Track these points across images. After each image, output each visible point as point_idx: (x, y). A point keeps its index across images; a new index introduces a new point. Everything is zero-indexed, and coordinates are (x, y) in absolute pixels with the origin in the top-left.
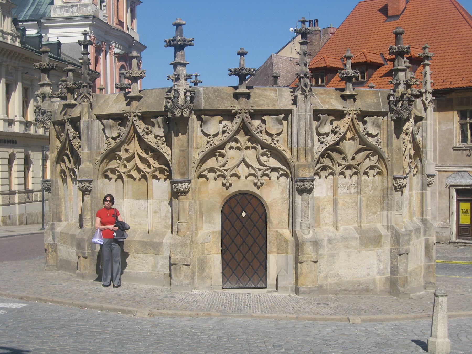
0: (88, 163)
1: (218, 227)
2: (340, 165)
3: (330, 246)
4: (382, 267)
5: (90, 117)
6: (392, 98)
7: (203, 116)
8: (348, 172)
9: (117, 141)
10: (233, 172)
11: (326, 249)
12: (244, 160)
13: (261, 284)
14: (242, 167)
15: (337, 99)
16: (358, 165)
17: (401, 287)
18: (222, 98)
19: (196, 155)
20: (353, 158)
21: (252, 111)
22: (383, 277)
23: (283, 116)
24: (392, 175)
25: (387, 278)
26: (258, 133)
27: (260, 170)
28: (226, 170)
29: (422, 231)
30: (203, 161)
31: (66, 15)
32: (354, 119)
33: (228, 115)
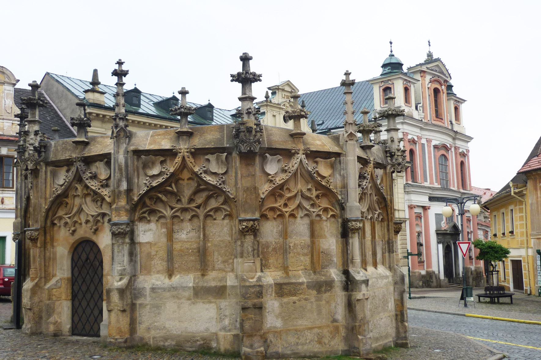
3: (154, 295)
4: (227, 322)
8: (188, 216)
11: (148, 299)
16: (197, 207)
17: (247, 347)
20: (191, 200)
22: (229, 333)
32: (186, 158)
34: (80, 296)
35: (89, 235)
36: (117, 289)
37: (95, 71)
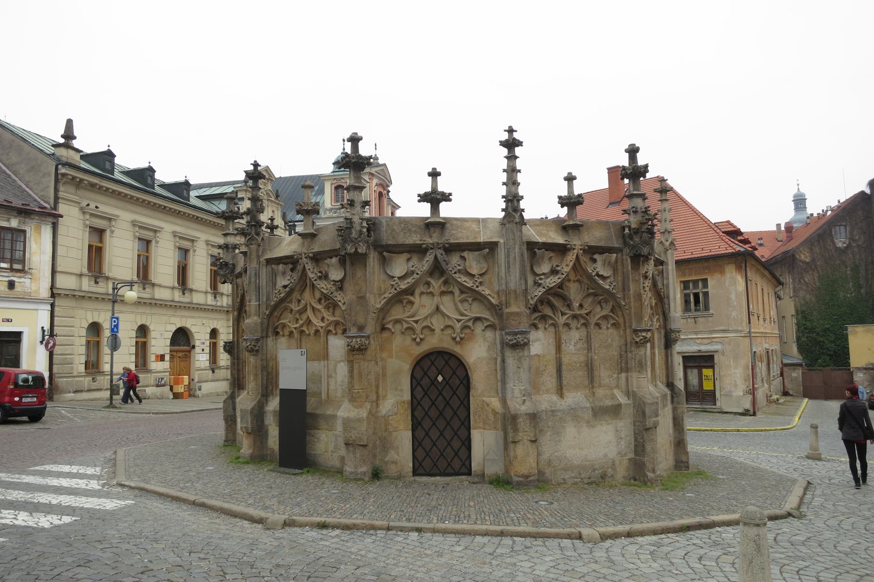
0: (256, 318)
1: (407, 396)
2: (563, 314)
5: (259, 263)
6: (627, 231)
7: (385, 254)
9: (287, 289)
10: (425, 324)
12: (438, 308)
13: (464, 470)
14: (436, 316)
15: (557, 232)
16: (587, 314)
18: (410, 230)
19: (376, 303)
20: (581, 306)
21: (447, 246)
23: (487, 250)
24: (630, 326)
25: (630, 460)
26: (455, 273)
27: (459, 321)
28: (416, 322)
29: (669, 398)
30: (384, 311)
31: (334, 215)
32: (580, 256)
33: (419, 250)
34: (427, 424)
35: (447, 344)
36: (526, 414)
37: (69, 123)
